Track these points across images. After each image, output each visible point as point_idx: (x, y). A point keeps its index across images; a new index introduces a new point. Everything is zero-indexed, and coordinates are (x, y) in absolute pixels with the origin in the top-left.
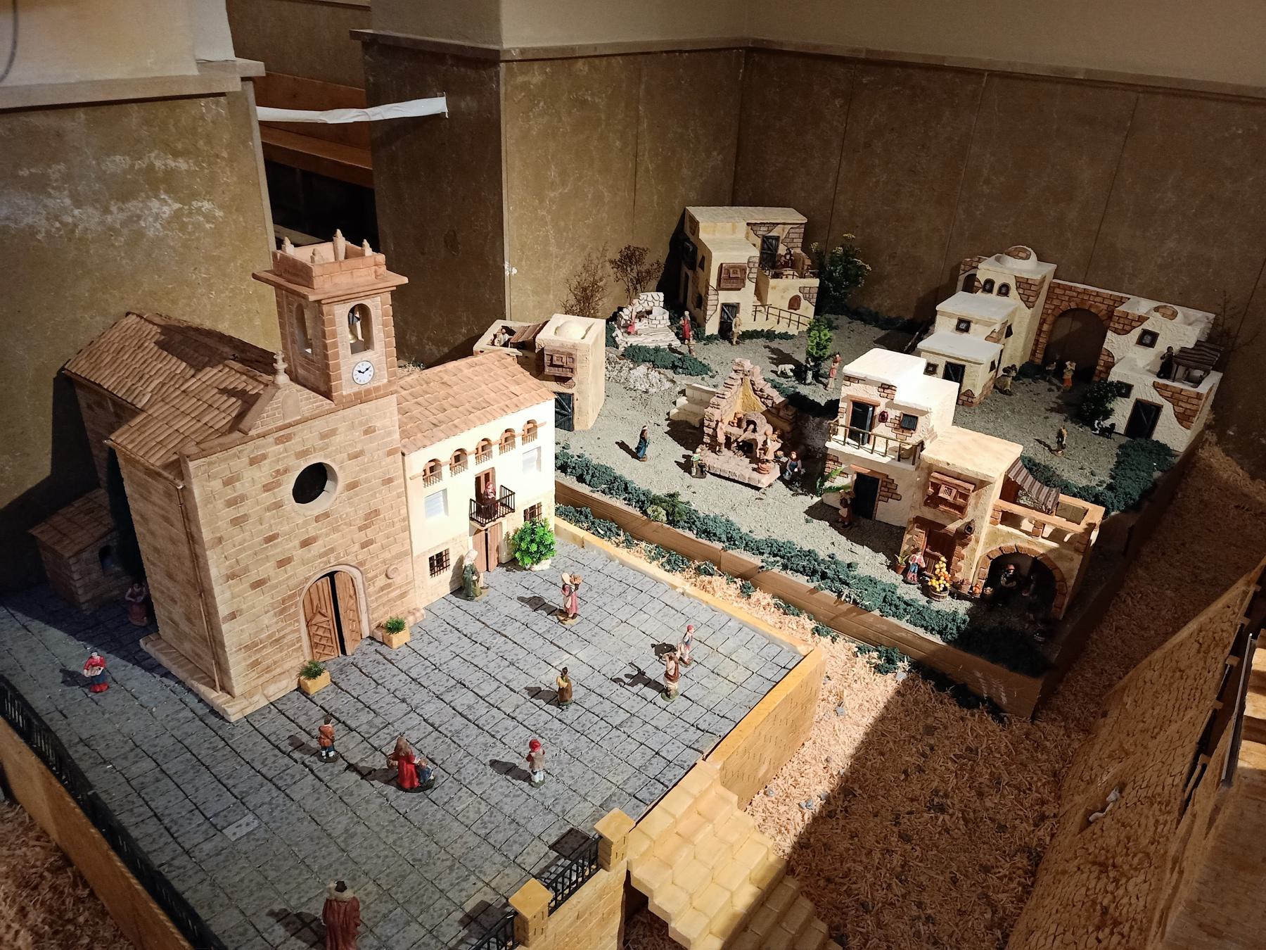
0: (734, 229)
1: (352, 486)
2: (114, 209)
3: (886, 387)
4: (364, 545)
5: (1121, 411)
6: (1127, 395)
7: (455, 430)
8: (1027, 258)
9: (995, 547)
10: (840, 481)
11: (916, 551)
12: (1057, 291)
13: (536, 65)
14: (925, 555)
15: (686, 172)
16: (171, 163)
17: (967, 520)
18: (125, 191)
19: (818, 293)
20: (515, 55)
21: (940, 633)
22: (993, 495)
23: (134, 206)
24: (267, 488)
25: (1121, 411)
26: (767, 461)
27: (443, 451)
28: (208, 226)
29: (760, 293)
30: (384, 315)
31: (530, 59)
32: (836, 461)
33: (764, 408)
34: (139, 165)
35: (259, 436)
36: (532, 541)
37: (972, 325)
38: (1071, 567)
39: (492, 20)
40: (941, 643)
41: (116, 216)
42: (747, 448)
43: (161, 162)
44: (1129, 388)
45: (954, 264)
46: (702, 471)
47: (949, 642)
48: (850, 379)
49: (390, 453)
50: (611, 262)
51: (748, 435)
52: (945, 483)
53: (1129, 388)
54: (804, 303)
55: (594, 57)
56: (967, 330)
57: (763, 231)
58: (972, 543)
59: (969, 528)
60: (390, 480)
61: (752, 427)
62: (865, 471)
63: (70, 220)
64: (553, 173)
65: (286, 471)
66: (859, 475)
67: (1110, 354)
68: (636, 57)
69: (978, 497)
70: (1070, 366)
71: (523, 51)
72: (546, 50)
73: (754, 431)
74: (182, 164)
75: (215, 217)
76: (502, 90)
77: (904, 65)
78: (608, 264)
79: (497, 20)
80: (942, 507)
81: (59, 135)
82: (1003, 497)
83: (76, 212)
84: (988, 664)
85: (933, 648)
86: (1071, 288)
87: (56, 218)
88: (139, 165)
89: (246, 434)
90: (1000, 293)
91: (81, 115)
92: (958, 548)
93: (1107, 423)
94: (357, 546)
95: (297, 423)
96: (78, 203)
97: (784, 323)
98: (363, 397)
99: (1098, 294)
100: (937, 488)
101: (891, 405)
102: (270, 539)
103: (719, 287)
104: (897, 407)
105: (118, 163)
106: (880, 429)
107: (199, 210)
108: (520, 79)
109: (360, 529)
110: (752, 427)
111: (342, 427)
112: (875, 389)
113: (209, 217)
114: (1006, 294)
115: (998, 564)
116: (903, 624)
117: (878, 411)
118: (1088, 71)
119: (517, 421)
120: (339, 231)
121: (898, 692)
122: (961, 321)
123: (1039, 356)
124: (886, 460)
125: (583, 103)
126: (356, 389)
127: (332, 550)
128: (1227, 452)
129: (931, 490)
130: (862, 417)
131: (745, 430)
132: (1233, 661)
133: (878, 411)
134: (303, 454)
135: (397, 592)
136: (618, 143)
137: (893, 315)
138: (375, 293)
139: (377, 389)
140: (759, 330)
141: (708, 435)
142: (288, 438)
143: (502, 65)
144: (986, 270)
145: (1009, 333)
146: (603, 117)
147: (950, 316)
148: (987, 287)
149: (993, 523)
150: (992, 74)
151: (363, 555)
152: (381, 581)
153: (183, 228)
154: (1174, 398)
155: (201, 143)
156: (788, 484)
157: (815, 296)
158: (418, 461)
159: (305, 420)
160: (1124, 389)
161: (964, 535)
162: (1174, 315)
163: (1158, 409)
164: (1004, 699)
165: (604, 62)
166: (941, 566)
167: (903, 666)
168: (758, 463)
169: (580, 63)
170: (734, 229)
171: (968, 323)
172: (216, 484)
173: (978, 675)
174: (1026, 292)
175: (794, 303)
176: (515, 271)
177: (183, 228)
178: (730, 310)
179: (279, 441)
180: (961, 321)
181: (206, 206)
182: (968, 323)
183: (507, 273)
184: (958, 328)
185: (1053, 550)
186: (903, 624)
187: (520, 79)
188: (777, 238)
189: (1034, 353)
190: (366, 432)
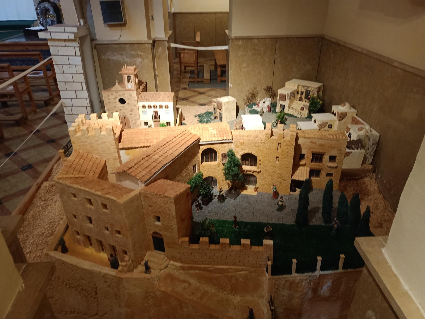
0: (294, 86)
1: (128, 104)
2: (132, 59)
4: (131, 114)
7: (149, 101)
13: (241, 40)
15: (294, 69)
16: (141, 53)
18: (133, 56)
20: (233, 38)
23: (135, 59)
24: (114, 99)
27: (146, 104)
28: (146, 64)
29: (291, 103)
30: (133, 78)
34: (136, 53)
35: (112, 91)
41: (132, 60)
43: (139, 53)
49: (135, 101)
50: (264, 89)
55: (259, 39)
57: (306, 88)
60: (135, 105)
63: (125, 60)
64: (245, 65)
65: (117, 98)
68: (275, 40)
71: (235, 37)
72: (242, 37)
74: (143, 54)
75: (147, 63)
78: (263, 90)
81: (125, 48)
83: (127, 59)
87: (124, 59)
88: (136, 53)
91: (128, 45)
94: (129, 114)
96: (127, 57)
98: (130, 90)
103: (279, 100)
105: (133, 52)
107: (145, 61)
108: (235, 43)
109: (130, 111)
111: (126, 94)
113: (147, 63)
119: (164, 104)
125: (255, 49)
126: (128, 88)
127: (124, 113)
134: (120, 96)
135: (137, 125)
136: (267, 60)
138: (131, 74)
139: (132, 89)
140: (290, 114)
142: (117, 93)
143: (231, 41)
146: (262, 53)
151: (130, 116)
152: (134, 122)
153: (142, 64)
155: (146, 51)
158: (141, 104)
159: (119, 91)
165: (263, 40)
169: (255, 40)
170: (294, 86)
172: (106, 96)
175: (302, 109)
176: (232, 86)
177: (142, 64)
178: (283, 107)
179: (116, 93)
181: (146, 61)
183: (230, 86)
187: (235, 43)
188: (310, 91)
190: (131, 96)
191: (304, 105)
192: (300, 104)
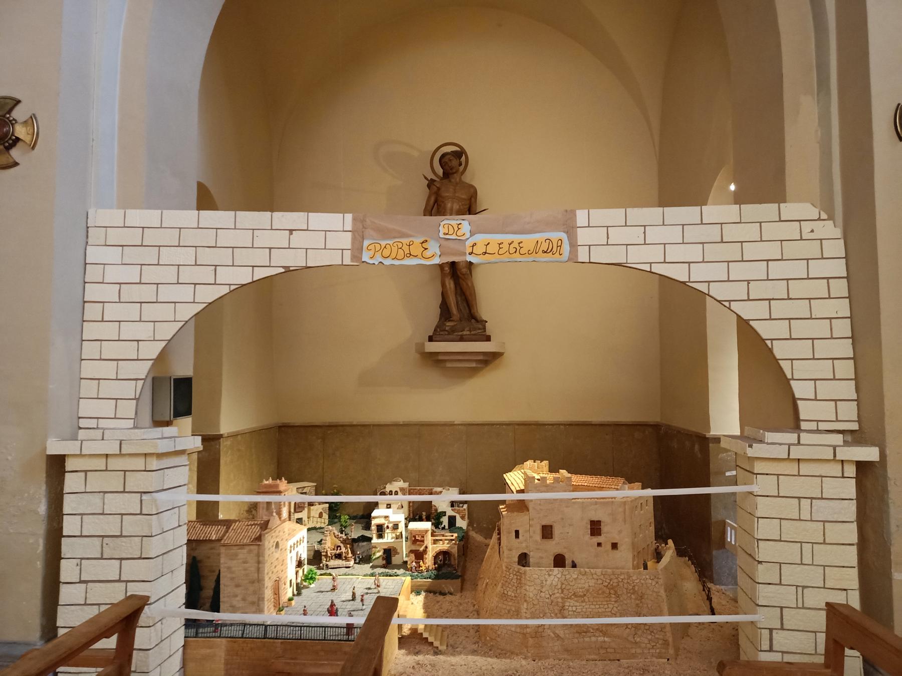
3: (386, 517)
5: (445, 521)
6: (445, 515)
8: (400, 481)
9: (434, 552)
10: (378, 555)
11: (412, 562)
12: (412, 491)
14: (415, 562)
17: (425, 545)
19: (329, 509)
21: (430, 578)
22: (429, 533)
25: (445, 521)
26: (349, 557)
31: (233, 436)
32: (375, 547)
33: (340, 542)
36: (313, 574)
37: (392, 505)
38: (455, 551)
39: (217, 425)
40: (431, 580)
42: (339, 556)
44: (445, 512)
45: (374, 490)
46: (327, 567)
47: (433, 579)
48: (374, 518)
51: (338, 552)
52: (417, 534)
53: (445, 512)
54: (324, 514)
56: (390, 507)
58: (428, 554)
59: (426, 547)
61: (339, 548)
62: (386, 547)
66: (385, 550)
67: (435, 506)
69: (426, 536)
70: (424, 514)
71: (228, 433)
72: (234, 432)
73: (340, 549)
76: (221, 447)
77: (342, 426)
79: (219, 423)
80: (418, 543)
82: (432, 536)
84: (445, 581)
85: (429, 583)
86: (415, 489)
89: (271, 529)
90: (395, 494)
92: (424, 556)
93: (443, 526)
95: (275, 528)
97: (319, 524)
99: (424, 489)
100: (415, 537)
101: (390, 522)
102: (272, 563)
104: (391, 522)
106: (388, 531)
108: (225, 443)
110: (339, 548)
112: (383, 519)
114: (397, 494)
115: (436, 557)
116: (419, 580)
117: (385, 526)
118: (403, 422)
120: (270, 478)
121: (425, 598)
122: (387, 505)
123: (411, 515)
124: (393, 540)
128: (476, 533)
129: (413, 539)
130: (380, 529)
131: (337, 550)
132: (499, 536)
133: (385, 526)
137: (355, 514)
141: (324, 555)
142: (275, 531)
144: (389, 488)
145: (402, 507)
147: (383, 504)
148: (391, 493)
149: (432, 545)
150: (374, 425)
154: (458, 512)
156: (358, 563)
157: (328, 511)
160: (444, 513)
161: (425, 551)
162: (449, 489)
163: (455, 517)
164: (452, 590)
166: (421, 563)
167: (423, 594)
168: (346, 559)
169: (239, 436)
171: (390, 505)
173: (444, 586)
174: (404, 492)
175: (321, 515)
180: (387, 505)
182: (390, 505)
184: (387, 508)
185: (449, 547)
186: (419, 580)
187: (225, 443)
189: (409, 514)
191: (323, 509)
192: (317, 510)
